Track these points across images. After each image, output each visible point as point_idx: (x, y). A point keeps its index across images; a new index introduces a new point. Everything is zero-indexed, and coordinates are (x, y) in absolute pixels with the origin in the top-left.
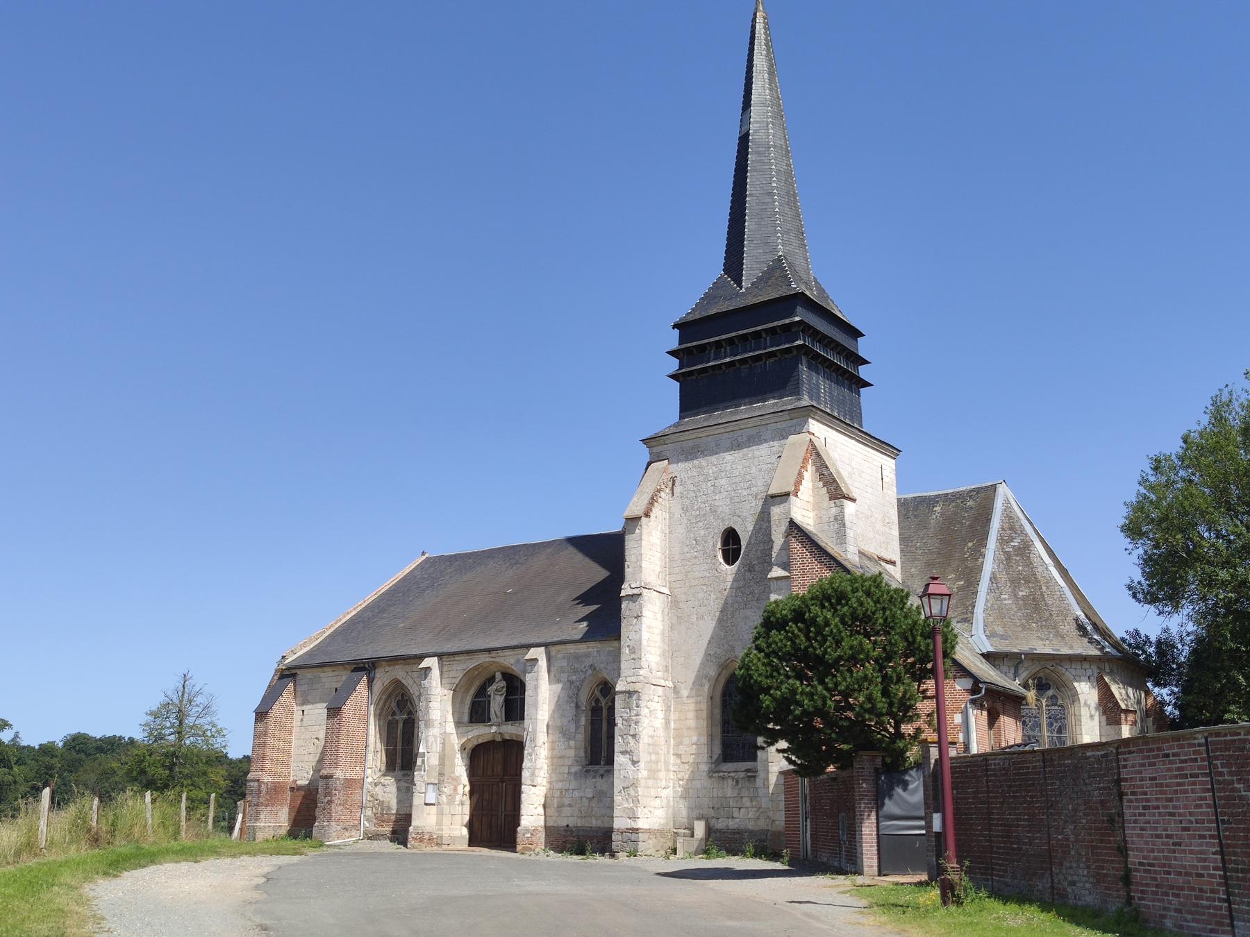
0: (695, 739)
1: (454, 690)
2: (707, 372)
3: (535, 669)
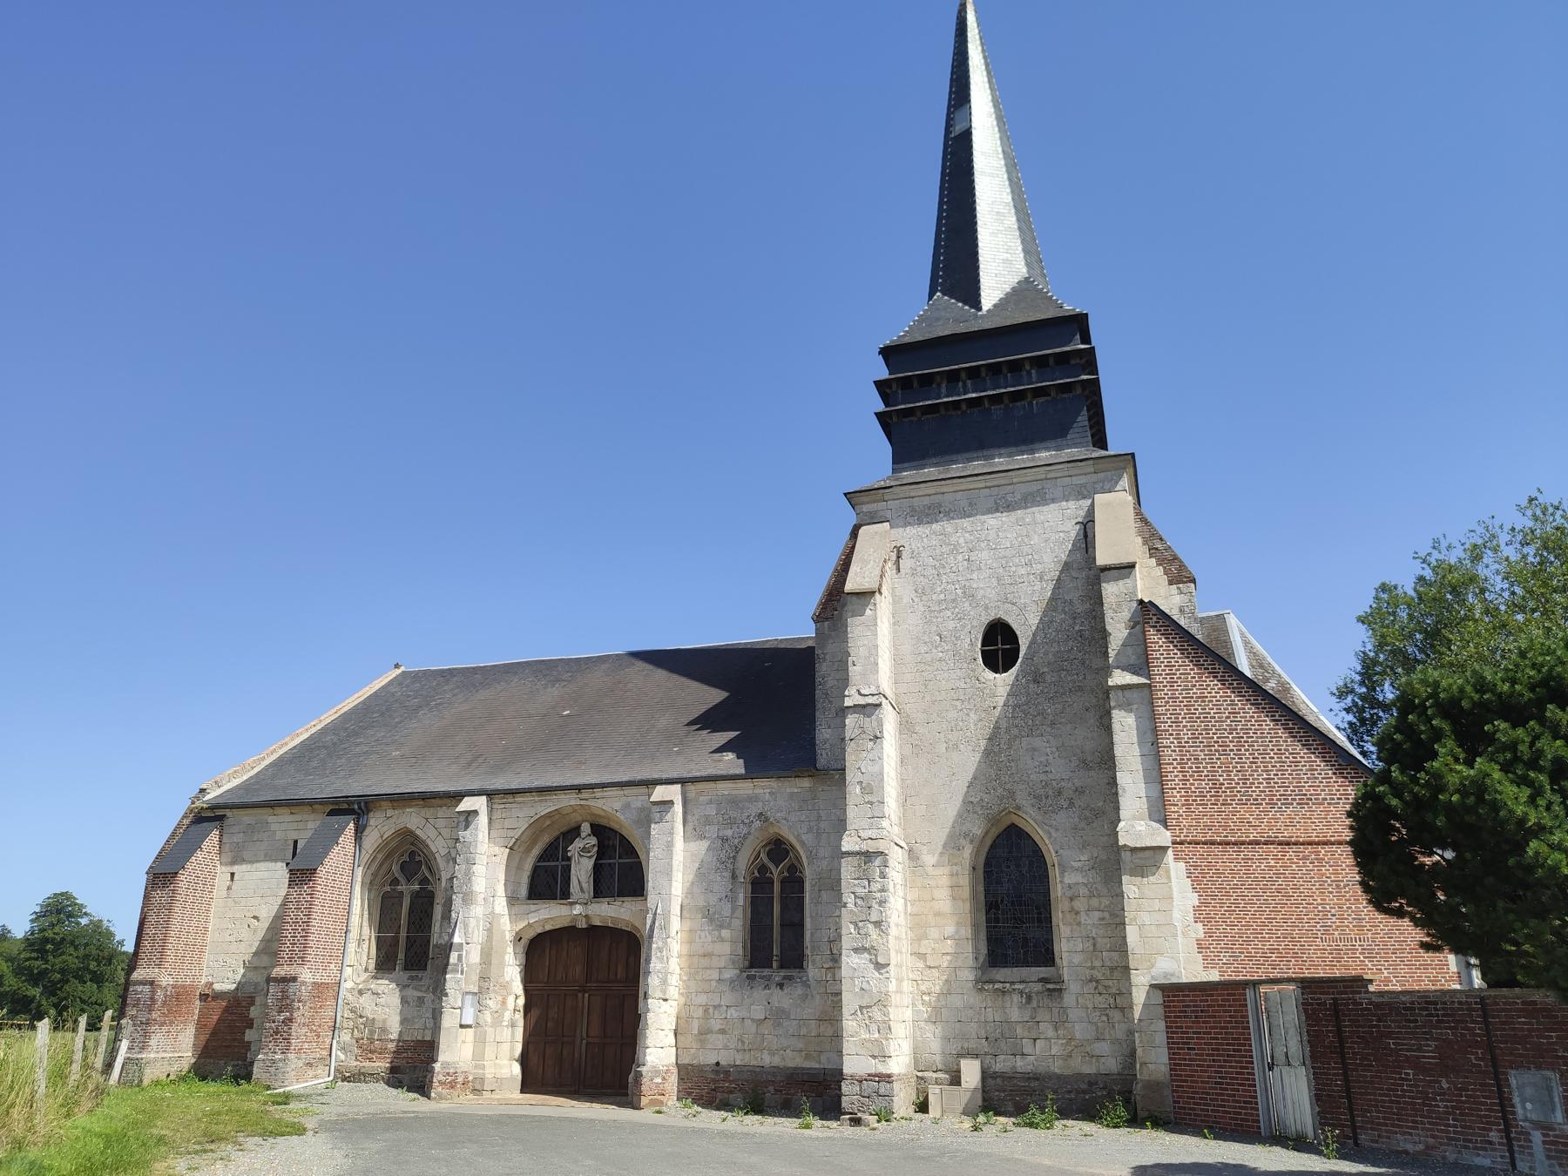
0: (950, 930)
1: (511, 849)
2: (938, 412)
3: (668, 817)
